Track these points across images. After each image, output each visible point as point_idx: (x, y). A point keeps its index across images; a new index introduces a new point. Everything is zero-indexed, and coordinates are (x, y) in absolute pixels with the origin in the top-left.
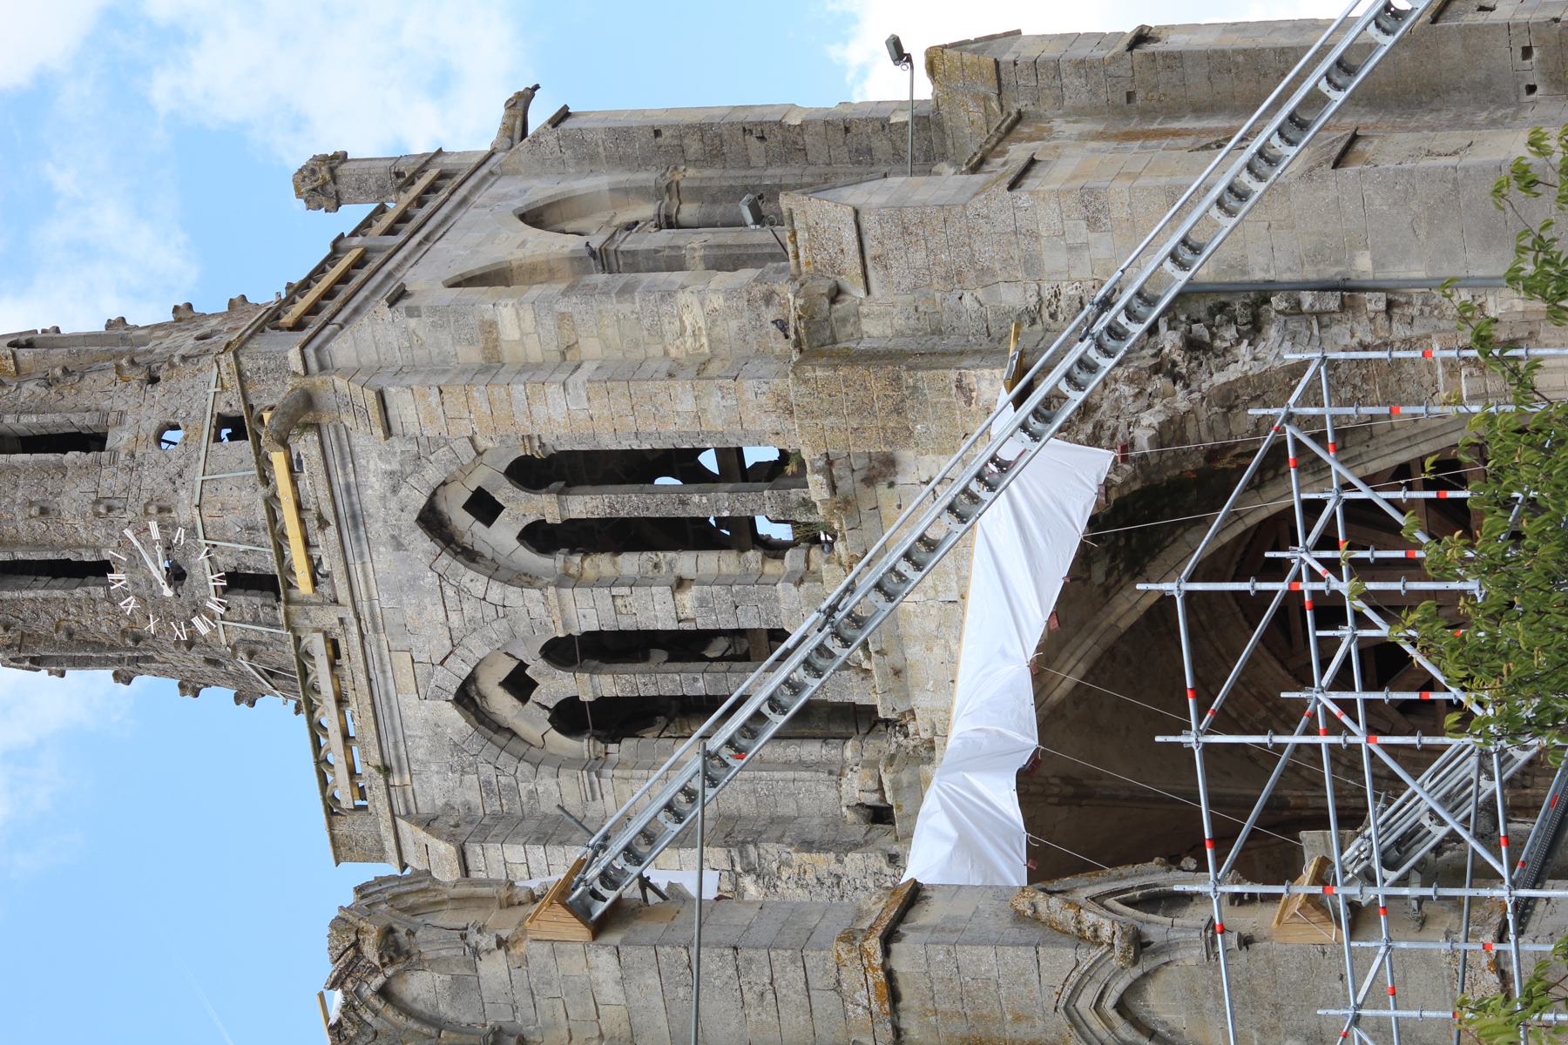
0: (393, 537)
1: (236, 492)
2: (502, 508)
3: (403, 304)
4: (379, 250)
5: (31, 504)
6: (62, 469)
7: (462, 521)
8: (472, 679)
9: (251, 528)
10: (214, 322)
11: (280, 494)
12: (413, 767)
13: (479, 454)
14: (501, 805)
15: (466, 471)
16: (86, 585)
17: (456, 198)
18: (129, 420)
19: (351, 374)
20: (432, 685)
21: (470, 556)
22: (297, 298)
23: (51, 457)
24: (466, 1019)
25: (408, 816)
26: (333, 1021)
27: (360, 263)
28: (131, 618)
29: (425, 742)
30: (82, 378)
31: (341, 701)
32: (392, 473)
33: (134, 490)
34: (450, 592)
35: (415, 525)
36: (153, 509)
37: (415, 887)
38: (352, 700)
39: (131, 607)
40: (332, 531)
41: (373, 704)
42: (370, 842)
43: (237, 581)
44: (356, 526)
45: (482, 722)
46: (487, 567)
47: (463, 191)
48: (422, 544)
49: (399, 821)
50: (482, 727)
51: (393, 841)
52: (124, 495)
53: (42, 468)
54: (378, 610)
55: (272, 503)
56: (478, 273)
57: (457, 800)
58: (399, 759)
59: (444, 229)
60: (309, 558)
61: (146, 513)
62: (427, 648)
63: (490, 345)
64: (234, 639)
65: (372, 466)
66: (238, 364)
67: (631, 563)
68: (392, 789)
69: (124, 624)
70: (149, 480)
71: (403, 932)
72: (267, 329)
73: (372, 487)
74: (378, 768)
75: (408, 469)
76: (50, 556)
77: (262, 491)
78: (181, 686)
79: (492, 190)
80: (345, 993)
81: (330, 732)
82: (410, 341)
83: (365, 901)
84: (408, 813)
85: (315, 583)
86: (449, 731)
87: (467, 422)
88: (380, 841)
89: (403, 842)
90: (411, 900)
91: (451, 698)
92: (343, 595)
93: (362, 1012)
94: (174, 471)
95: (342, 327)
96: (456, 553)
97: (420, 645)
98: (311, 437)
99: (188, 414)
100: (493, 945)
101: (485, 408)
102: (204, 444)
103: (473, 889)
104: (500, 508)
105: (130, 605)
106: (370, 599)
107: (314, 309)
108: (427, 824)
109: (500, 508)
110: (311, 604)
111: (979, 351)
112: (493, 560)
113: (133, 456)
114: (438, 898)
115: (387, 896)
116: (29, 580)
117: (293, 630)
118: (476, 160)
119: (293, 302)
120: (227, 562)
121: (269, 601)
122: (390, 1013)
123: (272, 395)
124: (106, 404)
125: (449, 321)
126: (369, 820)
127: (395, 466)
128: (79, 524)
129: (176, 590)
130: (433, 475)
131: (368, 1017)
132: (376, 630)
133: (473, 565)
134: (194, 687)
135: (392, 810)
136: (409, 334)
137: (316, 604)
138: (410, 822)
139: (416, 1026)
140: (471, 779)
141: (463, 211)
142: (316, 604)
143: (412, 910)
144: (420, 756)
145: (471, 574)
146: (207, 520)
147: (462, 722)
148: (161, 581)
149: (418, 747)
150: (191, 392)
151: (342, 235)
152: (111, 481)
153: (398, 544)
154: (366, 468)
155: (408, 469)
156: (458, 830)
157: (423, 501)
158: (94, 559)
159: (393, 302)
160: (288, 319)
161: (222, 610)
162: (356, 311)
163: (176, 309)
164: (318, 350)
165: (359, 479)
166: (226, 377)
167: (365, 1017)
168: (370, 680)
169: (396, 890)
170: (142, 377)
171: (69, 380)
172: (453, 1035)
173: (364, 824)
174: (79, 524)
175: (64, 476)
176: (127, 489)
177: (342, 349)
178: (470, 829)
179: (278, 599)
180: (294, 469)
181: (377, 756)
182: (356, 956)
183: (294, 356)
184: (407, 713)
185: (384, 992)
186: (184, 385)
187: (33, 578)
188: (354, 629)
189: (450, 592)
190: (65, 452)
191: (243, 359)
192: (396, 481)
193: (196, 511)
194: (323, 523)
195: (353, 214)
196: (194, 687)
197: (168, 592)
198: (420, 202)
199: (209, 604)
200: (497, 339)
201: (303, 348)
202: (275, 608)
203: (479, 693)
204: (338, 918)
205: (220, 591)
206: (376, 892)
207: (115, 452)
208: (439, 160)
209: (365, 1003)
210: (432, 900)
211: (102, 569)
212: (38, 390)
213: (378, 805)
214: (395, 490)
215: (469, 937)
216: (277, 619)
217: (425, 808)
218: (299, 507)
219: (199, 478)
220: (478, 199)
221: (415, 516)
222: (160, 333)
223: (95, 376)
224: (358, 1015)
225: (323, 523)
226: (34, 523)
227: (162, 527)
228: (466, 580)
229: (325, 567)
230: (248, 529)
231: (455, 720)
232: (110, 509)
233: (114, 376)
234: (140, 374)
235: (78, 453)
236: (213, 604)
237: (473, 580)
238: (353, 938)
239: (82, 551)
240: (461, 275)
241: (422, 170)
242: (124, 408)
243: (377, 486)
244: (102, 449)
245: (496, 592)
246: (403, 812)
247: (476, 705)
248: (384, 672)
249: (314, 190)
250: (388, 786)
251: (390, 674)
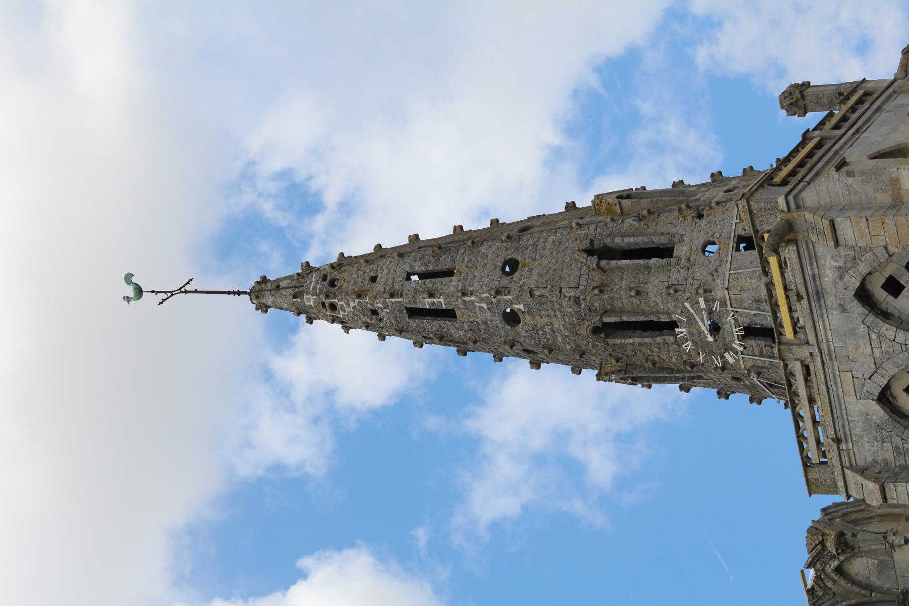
0: (841, 305)
1: (749, 280)
2: (904, 287)
3: (845, 169)
4: (830, 138)
5: (631, 289)
6: (648, 268)
7: (881, 295)
8: (887, 387)
9: (758, 301)
10: (734, 182)
11: (774, 281)
12: (854, 439)
13: (890, 256)
14: (906, 461)
15: (882, 266)
16: (663, 335)
17: (874, 107)
18: (687, 239)
19: (814, 211)
20: (865, 391)
21: (885, 315)
22: (783, 167)
23: (642, 261)
24: (887, 585)
25: (851, 467)
26: (809, 587)
27: (819, 146)
28: (689, 354)
30: (659, 215)
31: (811, 401)
32: (840, 268)
33: (690, 280)
34: (874, 337)
35: (853, 298)
36: (701, 291)
37: (856, 509)
38: (818, 400)
39: (689, 348)
40: (805, 302)
41: (830, 402)
42: (829, 483)
43: (750, 332)
44: (819, 299)
45: (893, 413)
46: (895, 322)
47: (878, 103)
48: (857, 308)
49: (846, 471)
50: (893, 415)
51: (842, 482)
52: (684, 283)
53: (637, 268)
54: (832, 347)
55: (770, 286)
56: (887, 150)
57: (880, 458)
58: (845, 434)
59: (868, 125)
60: (792, 318)
61: (697, 293)
62: (861, 369)
63: (896, 193)
64: (749, 365)
65: (828, 264)
66: (749, 206)
68: (842, 452)
69: (685, 357)
70: (698, 274)
71: (850, 535)
72: (765, 185)
73: (828, 276)
74: (833, 439)
75: (849, 265)
76: (642, 318)
77: (764, 279)
78: (718, 393)
79: (895, 102)
80: (816, 570)
81: (805, 419)
82: (849, 191)
83: (827, 517)
84: (851, 465)
85: (795, 332)
86: (874, 417)
87: (883, 237)
88: (834, 482)
89: (848, 483)
90: (854, 516)
91: (875, 398)
92: (812, 339)
93: (826, 581)
94: (712, 268)
95: (809, 184)
96: (878, 314)
97: (857, 367)
98: (792, 248)
99: (721, 236)
100: (902, 542)
101: (893, 229)
102: (730, 252)
103: (890, 510)
104: (903, 287)
105: (688, 346)
106: (828, 341)
107: (793, 173)
108: (862, 471)
109: (903, 287)
110: (793, 345)
112: (899, 317)
113: (689, 260)
114: (870, 515)
115: (840, 514)
116: (629, 333)
117: (783, 360)
118: (885, 84)
119: (781, 170)
120: (744, 321)
121: (769, 343)
122: (842, 582)
123: (769, 224)
124: (673, 230)
125: (871, 179)
126: (828, 470)
127: (841, 264)
128: (658, 300)
129: (715, 337)
130: (863, 268)
131: (830, 584)
132: (831, 359)
133: (887, 321)
134: (726, 394)
135: (842, 464)
136: (848, 187)
137: (796, 344)
138: (852, 470)
139: (858, 590)
140: (888, 445)
141: (879, 114)
142: (796, 344)
143: (855, 522)
144: (857, 432)
145: (886, 326)
146: (733, 297)
147: (882, 412)
148: (706, 332)
149: (857, 427)
150: (722, 223)
151: (808, 130)
152: (677, 275)
153: (843, 309)
154: (824, 265)
155: (849, 265)
156: (880, 476)
157: (858, 284)
158: (667, 320)
159: (838, 168)
160: (777, 179)
161: (742, 349)
162: (817, 174)
163: (712, 175)
164: (795, 197)
165: (820, 272)
166: (742, 214)
167: (828, 584)
168: (828, 389)
169: (845, 511)
170: (694, 214)
171: (652, 217)
172: (879, 595)
173: (825, 472)
174: (658, 300)
175: (649, 272)
176: (686, 279)
177: (810, 196)
178: (887, 474)
179: (774, 342)
180: (782, 266)
181: (833, 433)
182: (822, 549)
183: (781, 200)
184: (850, 407)
185: (839, 570)
186: (718, 218)
187: (632, 331)
188: (819, 359)
189: (874, 337)
190: (650, 259)
191: (752, 203)
192: (842, 273)
193: (726, 292)
194: (799, 298)
195: (813, 118)
196: (726, 394)
197: (710, 339)
198: (853, 109)
199: (734, 345)
200: (899, 189)
201: (786, 196)
202: (772, 347)
203: (892, 395)
204: (811, 527)
205: (740, 337)
206: (833, 512)
207: (679, 258)
208: (864, 85)
209: (828, 576)
210: (866, 516)
211: (672, 325)
212: (634, 223)
213: (833, 461)
214: (841, 277)
215: (888, 537)
216: (773, 353)
217: (861, 463)
218: (786, 289)
219: (728, 273)
220: (887, 107)
221: (853, 293)
222: (704, 189)
223: (666, 214)
224: (824, 583)
225: (799, 298)
226: (633, 299)
227: (706, 301)
228: (883, 330)
229: (801, 323)
230: (756, 301)
231: (877, 411)
232: (676, 291)
233: (677, 214)
234: (692, 213)
235: (657, 259)
236: (737, 345)
237: (888, 330)
238: (820, 538)
239: (661, 315)
240: (878, 152)
241: (854, 91)
242: (683, 233)
243: (830, 275)
244: (671, 256)
246: (848, 465)
247: (890, 402)
248: (836, 384)
249: (791, 104)
251: (839, 385)
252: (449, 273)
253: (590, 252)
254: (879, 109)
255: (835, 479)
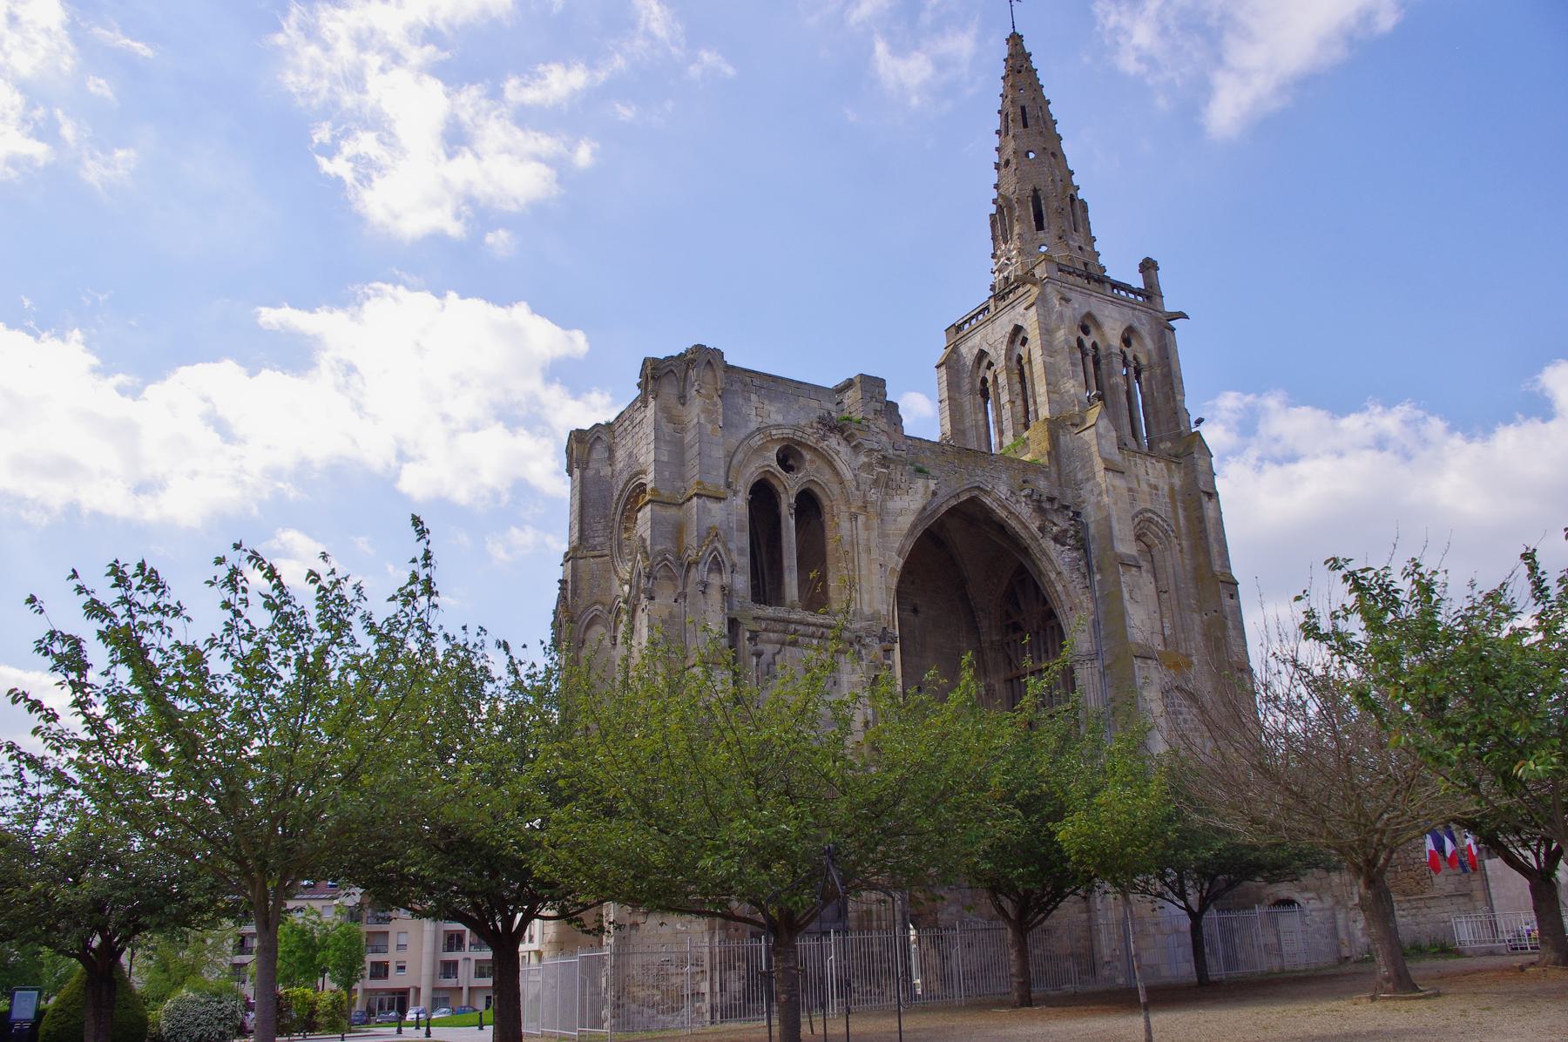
48: (1010, 328)
67: (1017, 387)
111: (1059, 470)
118: (1159, 308)
153: (1010, 321)
220: (1136, 312)
231: (976, 351)
245: (1003, 352)
252: (1025, 126)
253: (1035, 191)
254: (1135, 309)
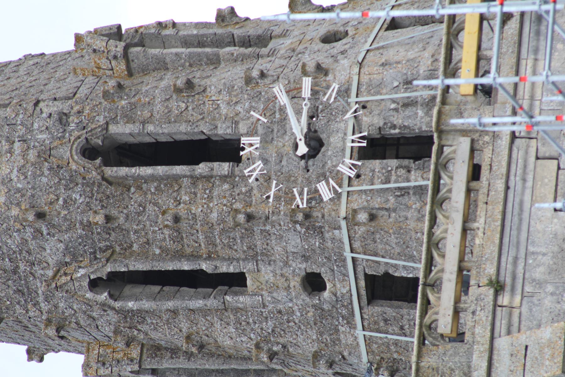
12: (528, 289)
29: (547, 260)
58: (514, 278)
68: (499, 309)
149: (539, 266)
168: (507, 188)
173: (456, 354)
219: (367, 47)
248: (524, 180)
250: (495, 305)
251: (529, 184)
255: (469, 367)
